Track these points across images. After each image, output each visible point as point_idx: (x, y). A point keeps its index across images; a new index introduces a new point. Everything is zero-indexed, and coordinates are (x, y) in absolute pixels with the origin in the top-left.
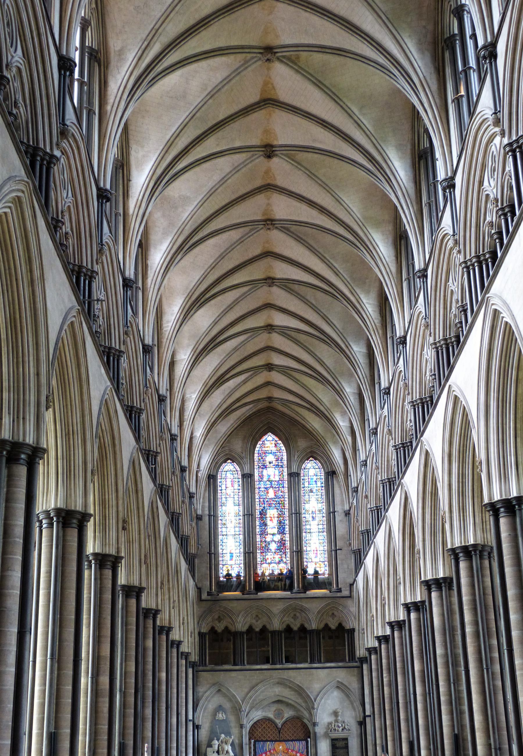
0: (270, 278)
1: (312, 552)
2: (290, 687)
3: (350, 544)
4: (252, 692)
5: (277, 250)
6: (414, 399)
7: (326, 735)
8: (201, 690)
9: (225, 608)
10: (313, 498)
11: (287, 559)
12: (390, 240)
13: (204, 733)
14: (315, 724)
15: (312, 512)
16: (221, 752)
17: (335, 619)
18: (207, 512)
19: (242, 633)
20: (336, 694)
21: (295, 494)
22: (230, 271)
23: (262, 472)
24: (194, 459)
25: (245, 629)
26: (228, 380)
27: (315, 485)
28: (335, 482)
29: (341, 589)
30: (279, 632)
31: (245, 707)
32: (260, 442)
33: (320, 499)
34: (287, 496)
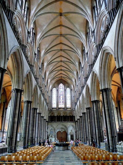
5: (62, 42)
7: (70, 134)
8: (48, 126)
12: (85, 34)
13: (49, 133)
20: (72, 127)
25: (56, 116)
31: (56, 129)
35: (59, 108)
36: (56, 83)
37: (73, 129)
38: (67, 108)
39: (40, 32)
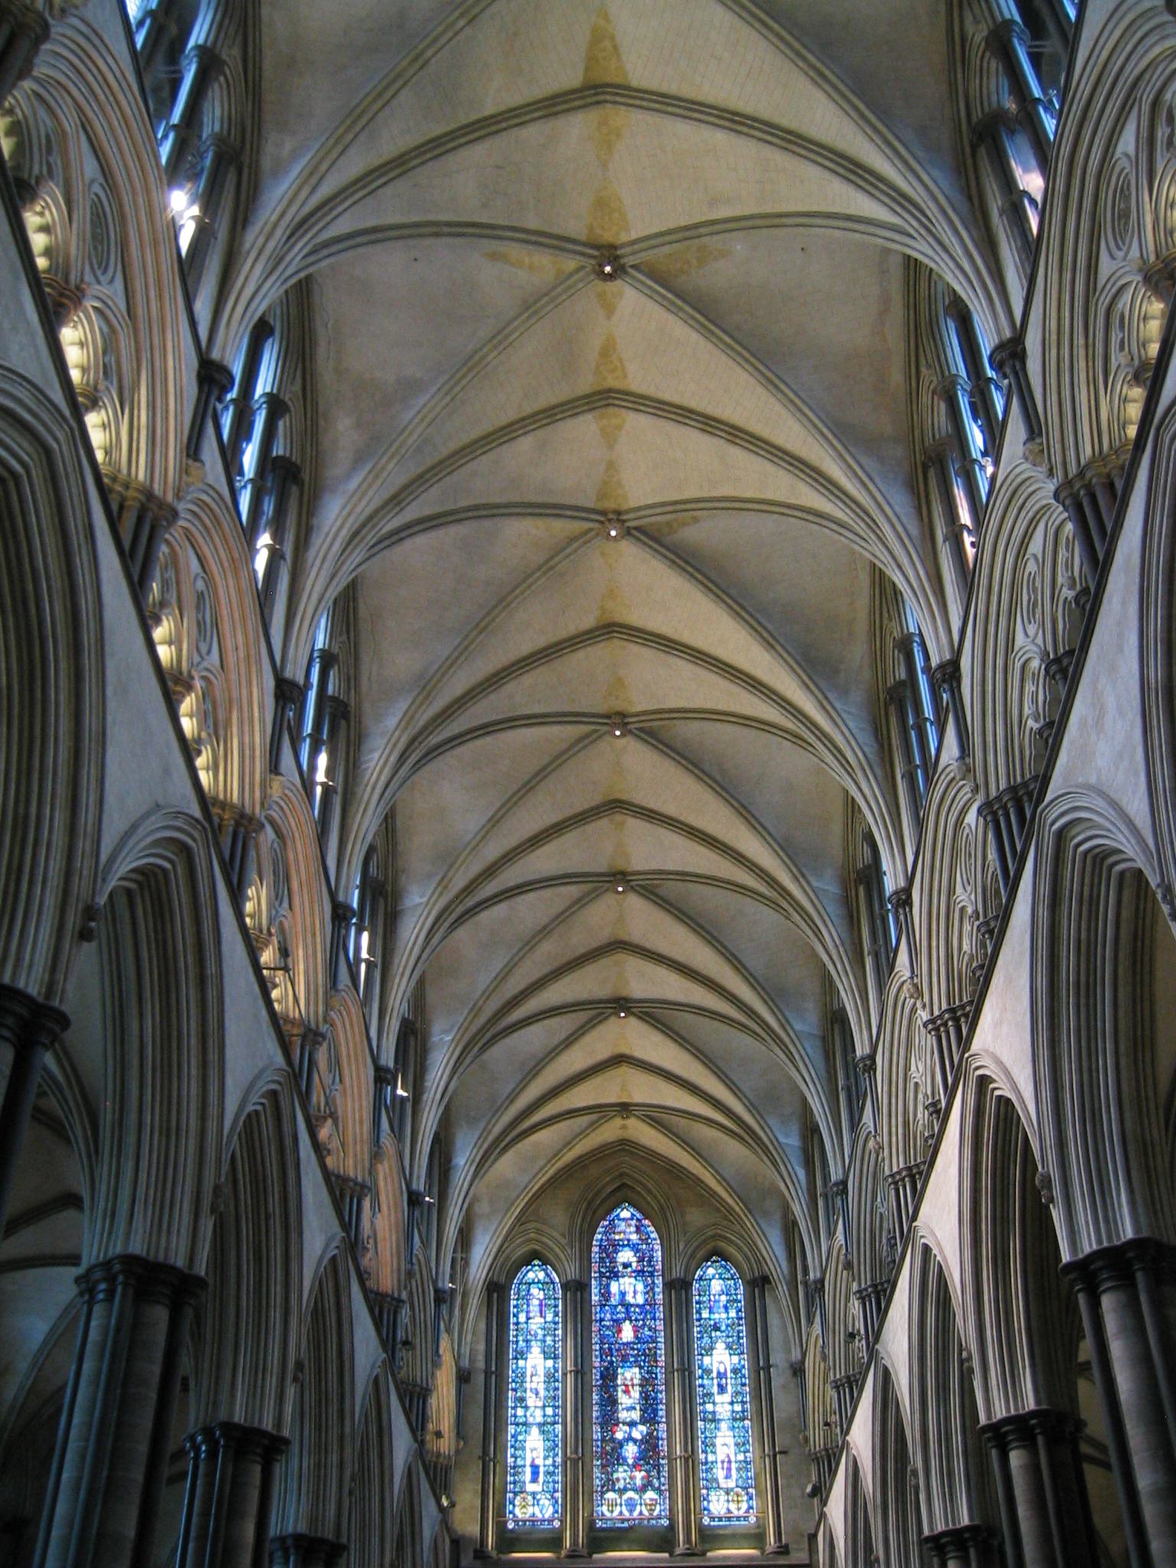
1: (719, 1465)
3: (806, 1440)
5: (635, 619)
6: (993, 793)
11: (662, 1479)
15: (719, 1373)
18: (481, 1364)
21: (680, 1326)
22: (524, 659)
23: (608, 1285)
24: (450, 1215)
27: (724, 1316)
29: (786, 1546)
35: (601, 1538)
38: (709, 1537)
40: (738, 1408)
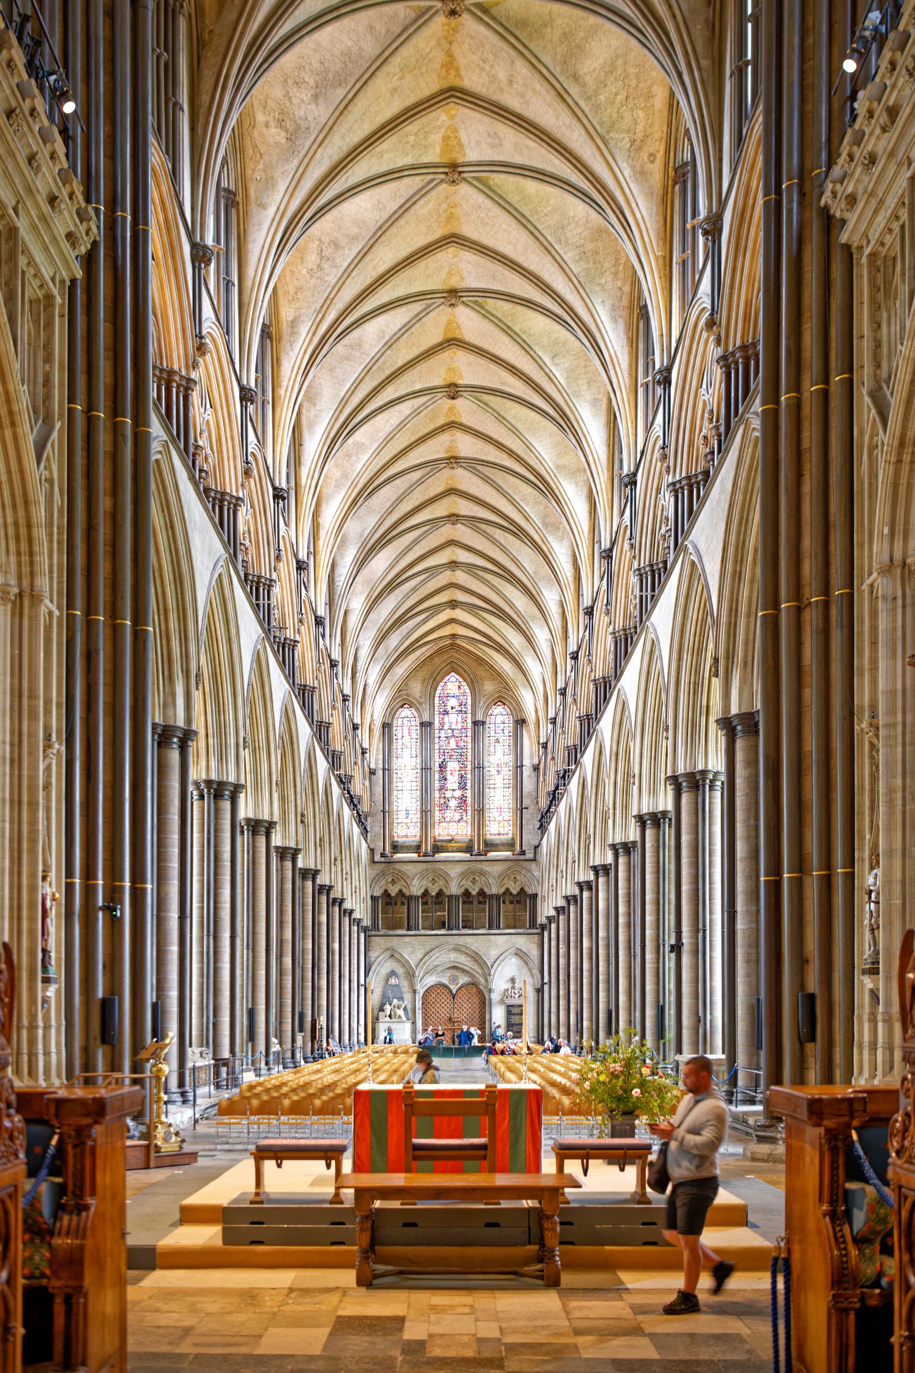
0: (453, 515)
2: (466, 954)
3: (537, 802)
4: (427, 958)
7: (502, 1001)
8: (373, 955)
9: (400, 871)
10: (500, 749)
14: (490, 991)
16: (393, 1016)
17: (518, 883)
19: (417, 898)
22: (409, 513)
25: (419, 893)
26: (406, 621)
28: (524, 732)
30: (457, 897)
31: (419, 973)
32: (442, 684)
33: (506, 751)
34: (469, 747)
36: (421, 675)
37: (525, 970)
38: (490, 846)
39: (338, 487)
40: (506, 782)
